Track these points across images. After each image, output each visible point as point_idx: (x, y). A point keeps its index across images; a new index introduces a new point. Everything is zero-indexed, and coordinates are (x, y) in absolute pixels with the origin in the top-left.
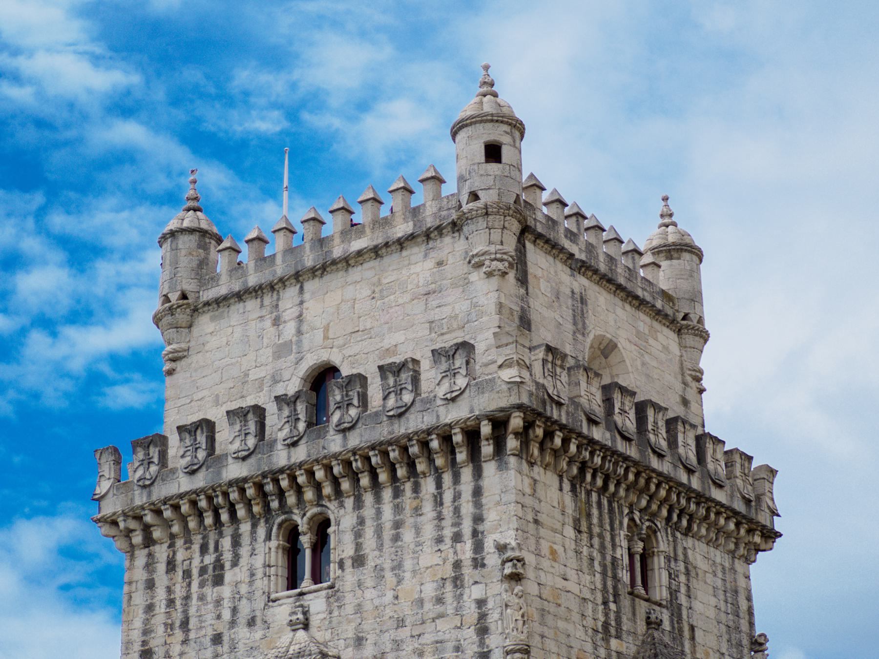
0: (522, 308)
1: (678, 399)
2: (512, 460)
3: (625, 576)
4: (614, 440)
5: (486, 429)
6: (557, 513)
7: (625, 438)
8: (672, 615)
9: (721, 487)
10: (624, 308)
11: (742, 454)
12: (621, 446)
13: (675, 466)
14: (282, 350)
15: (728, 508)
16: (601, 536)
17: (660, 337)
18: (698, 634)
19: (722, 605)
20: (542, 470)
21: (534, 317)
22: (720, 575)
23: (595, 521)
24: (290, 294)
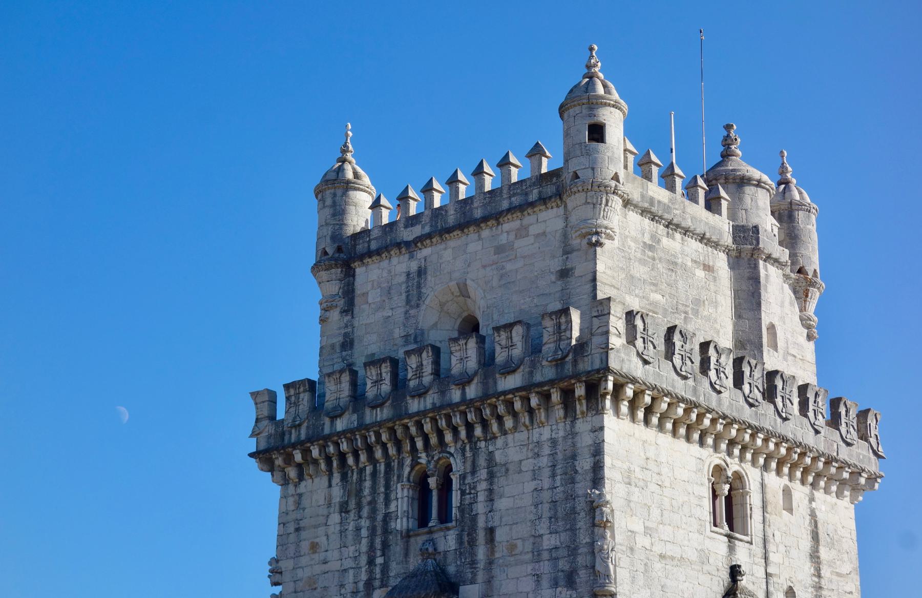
0: (346, 335)
1: (553, 278)
4: (361, 418)
6: (323, 511)
7: (374, 407)
8: (463, 531)
9: (514, 371)
10: (480, 238)
13: (443, 393)
17: (534, 230)
18: (500, 535)
19: (546, 483)
20: (310, 481)
21: (358, 333)
22: (546, 450)
23: (366, 492)
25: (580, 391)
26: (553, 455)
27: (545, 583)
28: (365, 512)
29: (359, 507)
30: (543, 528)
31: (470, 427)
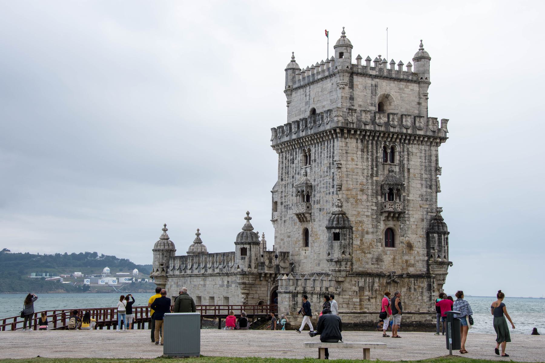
0: (351, 95)
2: (339, 139)
3: (381, 160)
4: (375, 127)
5: (333, 132)
6: (355, 149)
11: (432, 118)
12: (377, 128)
13: (401, 128)
14: (307, 103)
15: (422, 135)
16: (372, 152)
17: (410, 87)
19: (424, 161)
21: (355, 96)
22: (423, 152)
23: (370, 148)
24: (308, 88)
25: (438, 141)
26: (425, 154)
27: (424, 186)
28: (370, 153)
29: (368, 152)
30: (423, 172)
31: (405, 140)
